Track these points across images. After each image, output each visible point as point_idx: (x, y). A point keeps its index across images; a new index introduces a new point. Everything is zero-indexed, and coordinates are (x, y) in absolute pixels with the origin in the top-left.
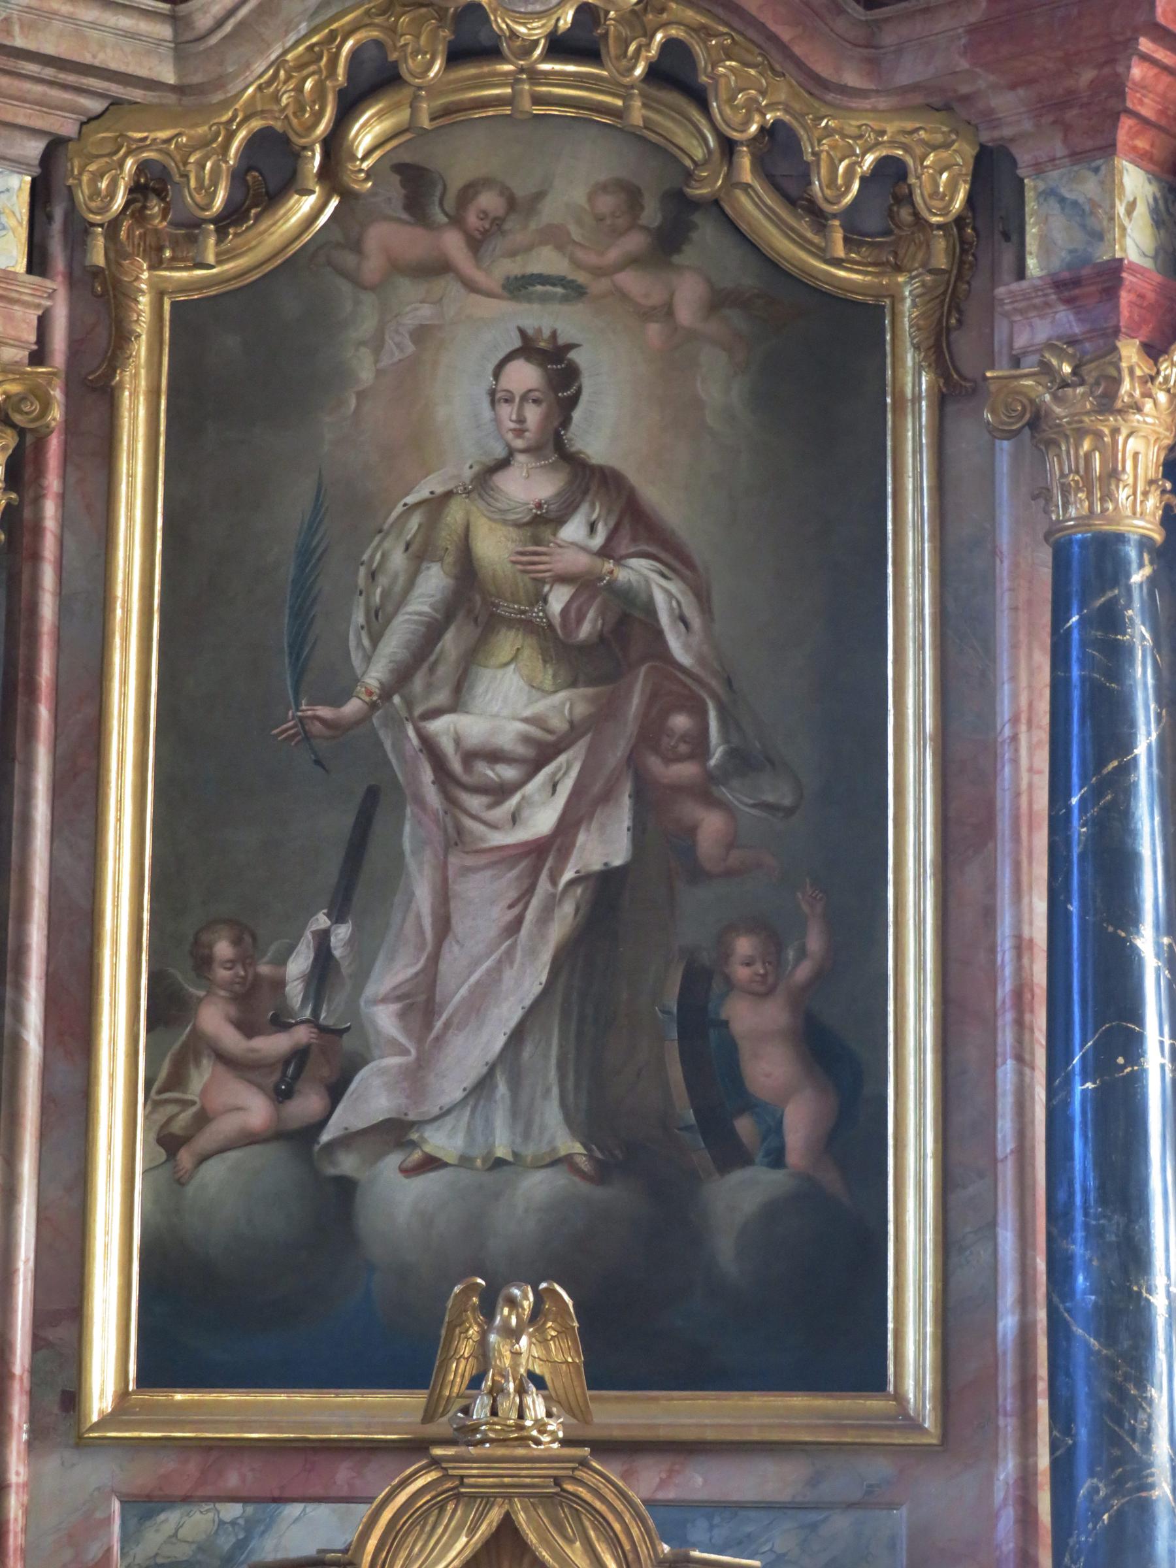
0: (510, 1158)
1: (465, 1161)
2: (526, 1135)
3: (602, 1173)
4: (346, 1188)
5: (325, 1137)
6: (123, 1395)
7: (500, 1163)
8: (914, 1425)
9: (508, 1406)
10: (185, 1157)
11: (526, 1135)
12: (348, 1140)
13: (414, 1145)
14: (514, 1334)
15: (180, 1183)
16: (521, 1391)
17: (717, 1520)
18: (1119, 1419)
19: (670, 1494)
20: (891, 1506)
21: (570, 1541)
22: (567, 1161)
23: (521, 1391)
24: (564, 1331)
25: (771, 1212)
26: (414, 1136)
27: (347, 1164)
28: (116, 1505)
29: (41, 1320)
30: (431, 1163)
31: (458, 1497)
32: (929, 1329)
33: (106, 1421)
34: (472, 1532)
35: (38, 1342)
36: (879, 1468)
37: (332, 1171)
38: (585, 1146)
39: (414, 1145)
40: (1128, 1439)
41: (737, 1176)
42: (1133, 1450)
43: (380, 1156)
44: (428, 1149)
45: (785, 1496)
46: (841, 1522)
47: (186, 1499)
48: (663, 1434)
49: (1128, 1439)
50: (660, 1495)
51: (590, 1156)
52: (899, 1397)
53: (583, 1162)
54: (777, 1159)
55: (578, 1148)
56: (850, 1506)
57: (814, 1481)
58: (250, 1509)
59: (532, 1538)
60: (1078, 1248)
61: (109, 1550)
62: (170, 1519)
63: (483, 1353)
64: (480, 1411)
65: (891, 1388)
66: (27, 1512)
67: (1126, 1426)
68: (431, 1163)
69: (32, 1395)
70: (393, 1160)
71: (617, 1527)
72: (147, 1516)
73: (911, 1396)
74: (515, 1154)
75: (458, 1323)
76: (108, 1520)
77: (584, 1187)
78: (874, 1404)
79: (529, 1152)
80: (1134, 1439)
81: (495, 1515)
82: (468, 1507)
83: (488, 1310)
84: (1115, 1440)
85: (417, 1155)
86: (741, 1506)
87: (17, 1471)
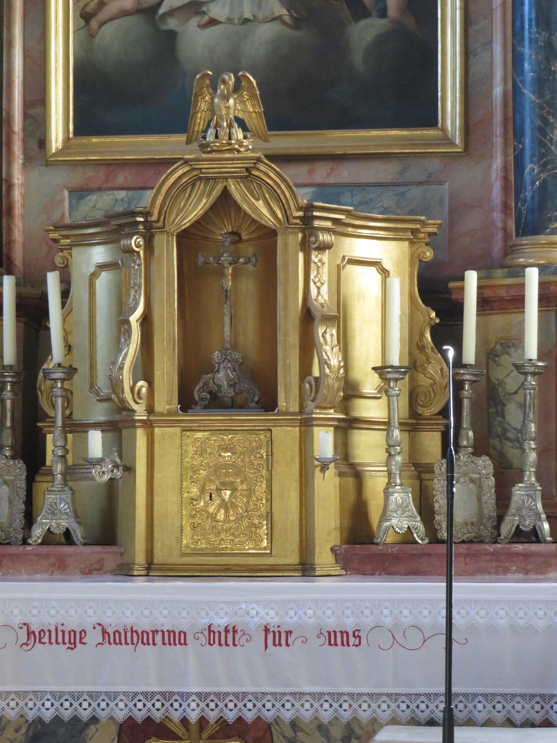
0: (251, 18)
1: (230, 20)
2: (259, 6)
3: (297, 24)
4: (172, 35)
5: (161, 11)
6: (67, 140)
7: (246, 21)
8: (452, 143)
9: (223, 133)
10: (94, 23)
11: (259, 6)
12: (171, 13)
13: (204, 13)
14: (226, 98)
15: (92, 36)
16: (230, 126)
17: (355, 192)
18: (544, 134)
19: (332, 180)
20: (440, 183)
21: (257, 200)
22: (279, 18)
23: (230, 126)
24: (252, 96)
25: (380, 40)
26: (204, 9)
27: (172, 24)
28: (66, 193)
29: (27, 105)
30: (213, 22)
31: (200, 179)
32: (458, 95)
33: (59, 152)
34: (209, 195)
35: (26, 116)
36: (435, 165)
37: (165, 28)
38: (288, 11)
39: (204, 13)
40: (549, 144)
41: (363, 23)
42: (551, 150)
43: (189, 19)
44: (212, 15)
45: (388, 180)
46: (415, 192)
47: (99, 189)
48: (326, 151)
49: (549, 144)
50: (328, 181)
51: (291, 15)
52: (444, 129)
53: (287, 19)
54: (383, 13)
55: (285, 12)
56: (420, 183)
57: (401, 173)
58: (130, 193)
59: (238, 198)
60: (527, 51)
61: (63, 215)
62: (92, 199)
63: (212, 108)
64: (210, 137)
65: (440, 125)
66: (24, 196)
67: (548, 137)
68: (213, 22)
69: (24, 141)
70: (195, 21)
71: (278, 191)
72: (81, 198)
73: (450, 128)
74: (254, 16)
75: (199, 94)
76: (62, 201)
77: (288, 31)
78: (431, 132)
79: (261, 15)
80: (552, 145)
81: (219, 188)
82: (206, 184)
83: (215, 88)
84: (542, 144)
85: (206, 19)
86: (367, 185)
87: (18, 177)
